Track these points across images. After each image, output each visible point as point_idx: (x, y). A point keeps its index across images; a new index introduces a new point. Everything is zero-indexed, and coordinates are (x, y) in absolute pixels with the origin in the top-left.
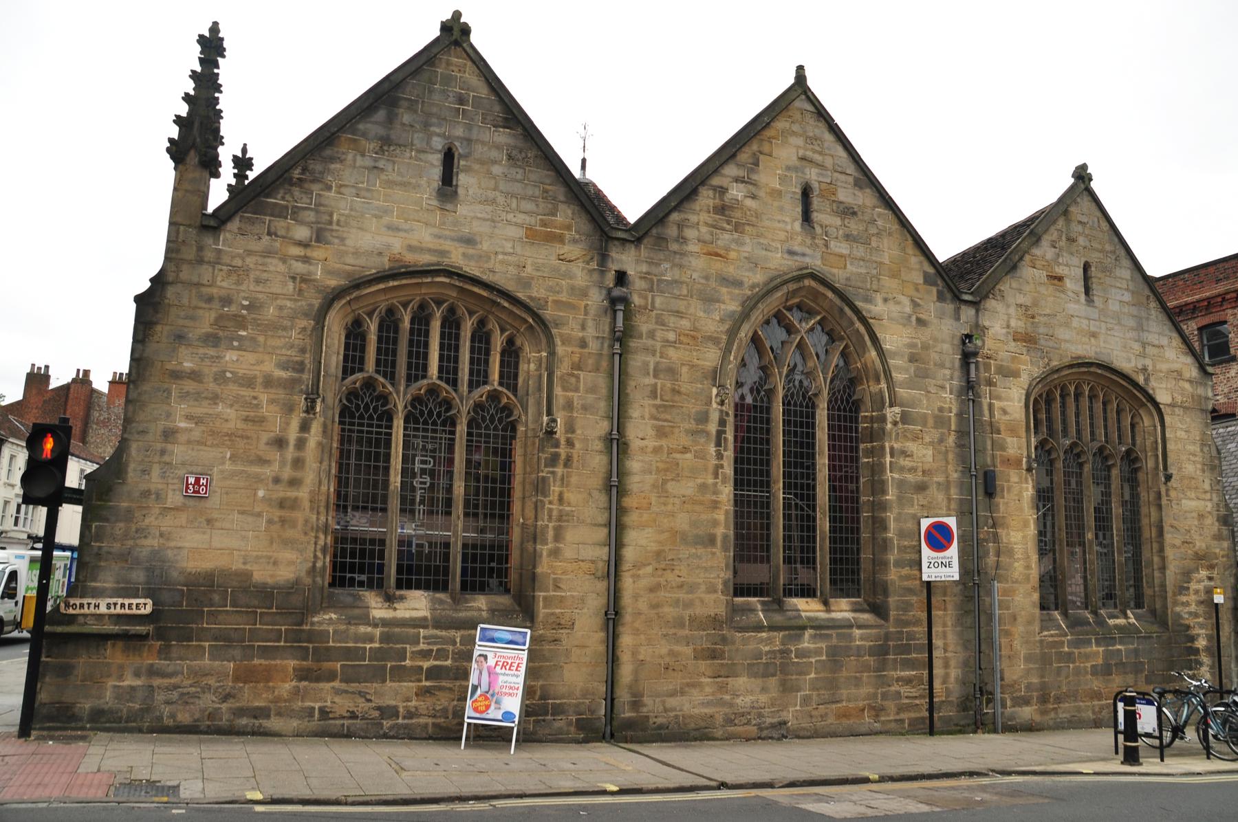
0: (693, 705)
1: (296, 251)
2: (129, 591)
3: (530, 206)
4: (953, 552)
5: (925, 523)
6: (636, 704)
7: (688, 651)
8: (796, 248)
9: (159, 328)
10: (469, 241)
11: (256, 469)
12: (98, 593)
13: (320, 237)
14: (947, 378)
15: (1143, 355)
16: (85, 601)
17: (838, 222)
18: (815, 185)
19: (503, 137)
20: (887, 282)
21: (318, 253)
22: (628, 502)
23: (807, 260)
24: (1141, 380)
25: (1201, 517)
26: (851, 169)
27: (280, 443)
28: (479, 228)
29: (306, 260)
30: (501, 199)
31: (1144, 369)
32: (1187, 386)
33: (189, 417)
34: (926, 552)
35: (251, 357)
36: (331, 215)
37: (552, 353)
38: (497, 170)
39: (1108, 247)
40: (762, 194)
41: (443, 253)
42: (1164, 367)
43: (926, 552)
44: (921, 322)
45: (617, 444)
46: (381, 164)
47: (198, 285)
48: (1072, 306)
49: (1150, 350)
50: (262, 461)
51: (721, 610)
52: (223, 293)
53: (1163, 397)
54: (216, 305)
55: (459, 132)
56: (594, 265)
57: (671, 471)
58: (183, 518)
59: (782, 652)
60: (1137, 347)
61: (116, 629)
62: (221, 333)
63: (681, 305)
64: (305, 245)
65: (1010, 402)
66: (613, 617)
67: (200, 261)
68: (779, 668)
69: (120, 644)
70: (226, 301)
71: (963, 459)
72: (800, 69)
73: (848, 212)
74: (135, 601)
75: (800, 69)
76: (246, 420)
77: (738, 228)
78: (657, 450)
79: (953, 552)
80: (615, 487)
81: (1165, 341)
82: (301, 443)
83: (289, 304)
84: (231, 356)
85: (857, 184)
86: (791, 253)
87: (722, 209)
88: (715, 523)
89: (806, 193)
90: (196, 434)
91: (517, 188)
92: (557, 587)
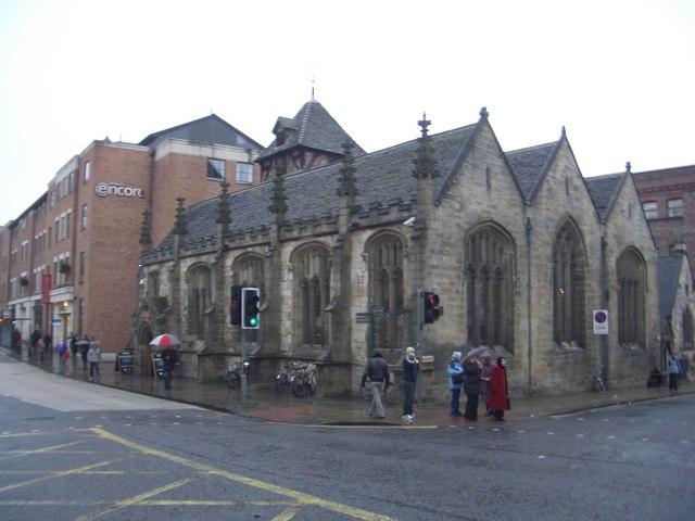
1: (456, 214)
4: (606, 323)
5: (595, 312)
10: (494, 207)
14: (599, 253)
21: (462, 215)
22: (533, 308)
28: (496, 202)
29: (459, 217)
34: (595, 323)
37: (516, 252)
41: (489, 213)
45: (529, 286)
50: (454, 300)
51: (551, 347)
66: (530, 353)
73: (576, 188)
75: (564, 128)
80: (529, 303)
87: (549, 190)
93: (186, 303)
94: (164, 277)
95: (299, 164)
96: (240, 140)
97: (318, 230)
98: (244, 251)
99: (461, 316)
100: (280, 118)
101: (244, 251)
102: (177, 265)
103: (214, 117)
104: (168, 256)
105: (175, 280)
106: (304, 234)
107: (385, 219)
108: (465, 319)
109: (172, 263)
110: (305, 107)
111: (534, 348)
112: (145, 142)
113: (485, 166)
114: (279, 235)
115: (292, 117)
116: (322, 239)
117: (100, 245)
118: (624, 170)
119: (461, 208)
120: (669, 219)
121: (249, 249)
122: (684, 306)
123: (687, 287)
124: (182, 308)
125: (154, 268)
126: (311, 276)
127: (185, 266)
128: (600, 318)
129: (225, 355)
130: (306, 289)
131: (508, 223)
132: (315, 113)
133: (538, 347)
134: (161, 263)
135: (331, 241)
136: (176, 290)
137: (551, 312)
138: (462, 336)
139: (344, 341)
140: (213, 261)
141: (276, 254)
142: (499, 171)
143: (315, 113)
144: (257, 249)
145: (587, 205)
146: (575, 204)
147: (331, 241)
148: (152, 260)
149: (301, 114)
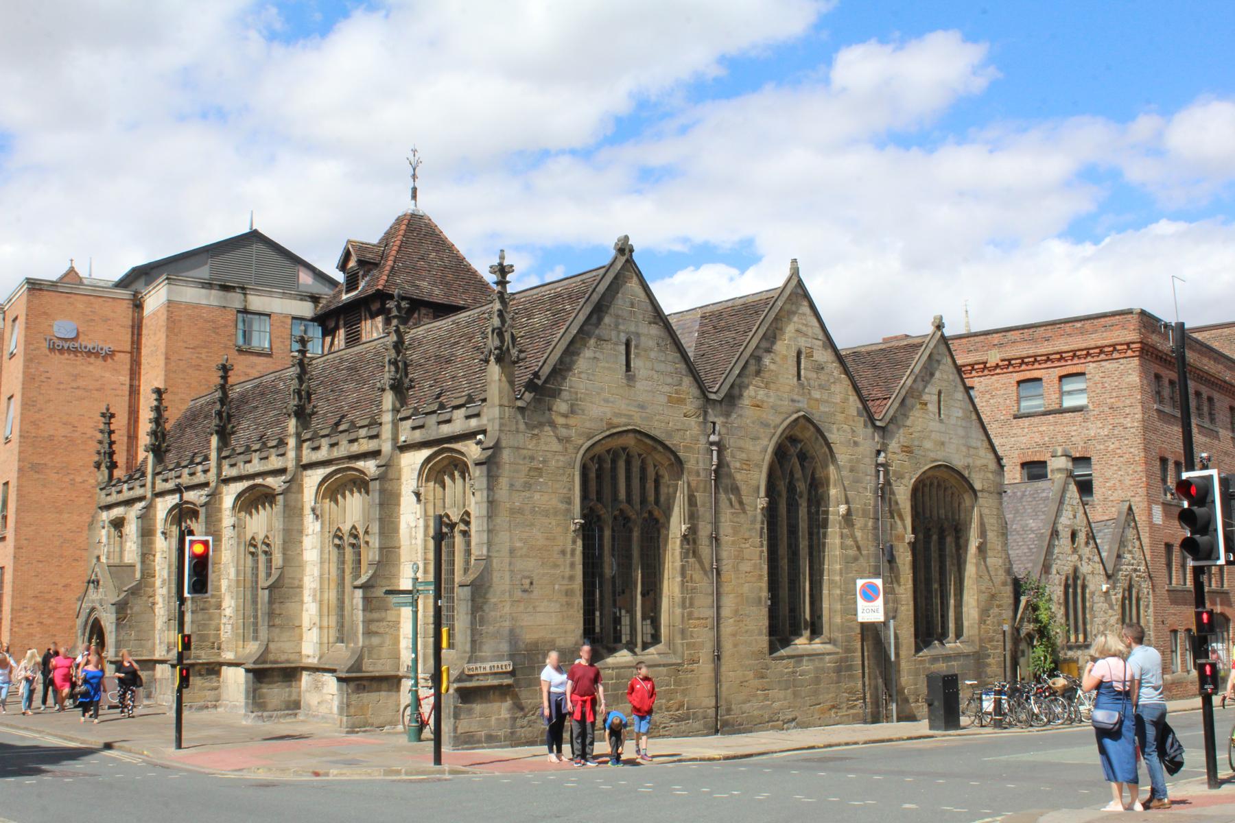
0: (753, 708)
2: (500, 658)
3: (669, 380)
6: (729, 711)
7: (751, 674)
8: (796, 397)
9: (501, 480)
10: (642, 407)
11: (552, 571)
12: (483, 660)
13: (573, 412)
15: (969, 456)
16: (478, 665)
17: (815, 376)
18: (803, 350)
19: (655, 330)
20: (840, 417)
21: (571, 421)
23: (800, 405)
24: (966, 475)
25: (996, 570)
26: (821, 336)
27: (563, 552)
29: (567, 426)
30: (655, 376)
31: (968, 466)
32: (990, 476)
33: (521, 540)
35: (546, 497)
36: (576, 393)
38: (652, 355)
39: (951, 377)
40: (777, 359)
41: (630, 417)
42: (979, 463)
43: (861, 604)
44: (856, 444)
46: (597, 355)
47: (518, 448)
48: (932, 424)
49: (972, 451)
50: (556, 566)
52: (530, 453)
53: (977, 486)
54: (527, 461)
55: (633, 329)
56: (701, 419)
57: (740, 558)
58: (522, 607)
59: (793, 672)
60: (964, 449)
61: (496, 682)
62: (532, 481)
63: (741, 443)
64: (566, 416)
65: (903, 494)
67: (518, 432)
68: (790, 683)
69: (497, 693)
70: (532, 458)
71: (876, 538)
72: (794, 261)
73: (820, 368)
74: (504, 663)
75: (794, 261)
76: (547, 539)
77: (767, 386)
78: (734, 543)
79: (880, 602)
81: (979, 444)
82: (573, 552)
83: (562, 458)
84: (537, 496)
85: (824, 347)
86: (793, 401)
88: (761, 589)
89: (799, 354)
90: (524, 551)
91: (662, 367)
92: (692, 637)
93: (165, 574)
94: (132, 528)
95: (380, 325)
96: (305, 278)
97: (355, 448)
98: (251, 483)
99: (569, 593)
100: (349, 241)
101: (251, 483)
102: (150, 507)
103: (254, 237)
104: (139, 492)
105: (146, 533)
106: (336, 453)
107: (446, 430)
108: (579, 600)
109: (143, 504)
110: (399, 221)
111: (727, 646)
112: (124, 283)
113: (623, 338)
114: (299, 458)
115: (375, 241)
116: (360, 464)
117: (36, 468)
118: (930, 329)
119: (573, 412)
120: (1063, 411)
121: (259, 481)
122: (1068, 569)
123: (1074, 535)
124: (158, 583)
125: (117, 512)
126: (346, 528)
127: (163, 507)
128: (870, 595)
129: (221, 664)
130: (439, 538)
131: (669, 434)
132: (417, 232)
133: (735, 646)
134: (129, 503)
135: (370, 467)
136: (146, 554)
137: (764, 584)
138: (572, 627)
139: (388, 641)
140: (204, 500)
141: (294, 487)
142: (651, 343)
143: (417, 232)
144: (270, 481)
145: (841, 389)
146: (816, 394)
147: (370, 467)
148: (114, 498)
149: (388, 236)
